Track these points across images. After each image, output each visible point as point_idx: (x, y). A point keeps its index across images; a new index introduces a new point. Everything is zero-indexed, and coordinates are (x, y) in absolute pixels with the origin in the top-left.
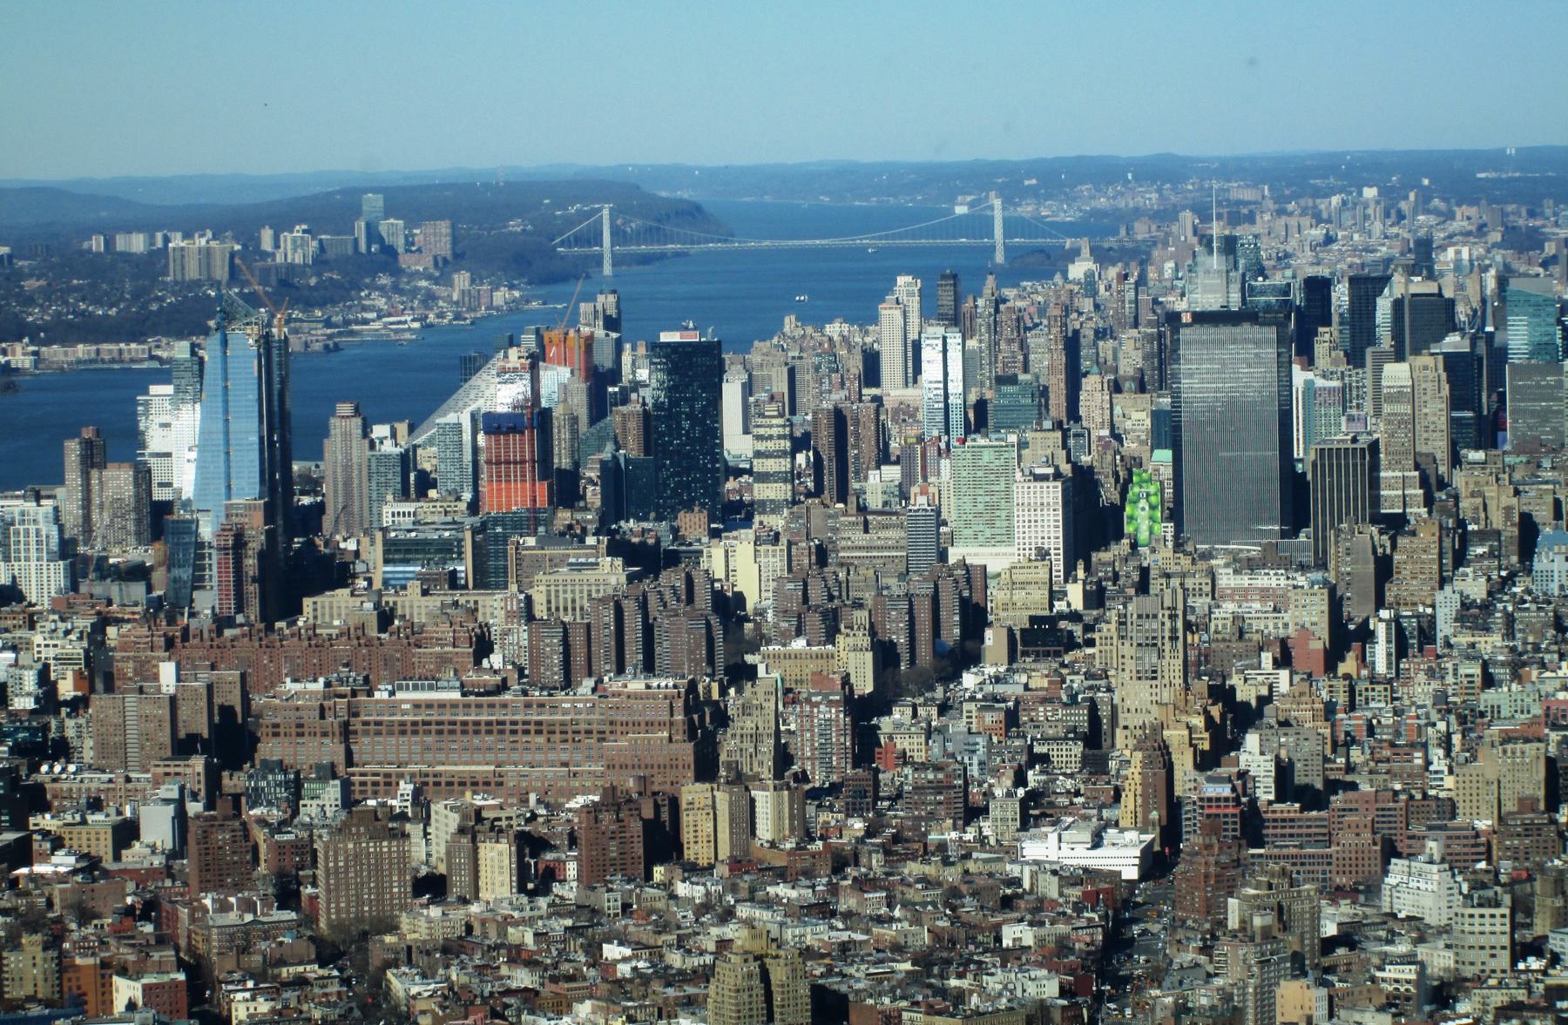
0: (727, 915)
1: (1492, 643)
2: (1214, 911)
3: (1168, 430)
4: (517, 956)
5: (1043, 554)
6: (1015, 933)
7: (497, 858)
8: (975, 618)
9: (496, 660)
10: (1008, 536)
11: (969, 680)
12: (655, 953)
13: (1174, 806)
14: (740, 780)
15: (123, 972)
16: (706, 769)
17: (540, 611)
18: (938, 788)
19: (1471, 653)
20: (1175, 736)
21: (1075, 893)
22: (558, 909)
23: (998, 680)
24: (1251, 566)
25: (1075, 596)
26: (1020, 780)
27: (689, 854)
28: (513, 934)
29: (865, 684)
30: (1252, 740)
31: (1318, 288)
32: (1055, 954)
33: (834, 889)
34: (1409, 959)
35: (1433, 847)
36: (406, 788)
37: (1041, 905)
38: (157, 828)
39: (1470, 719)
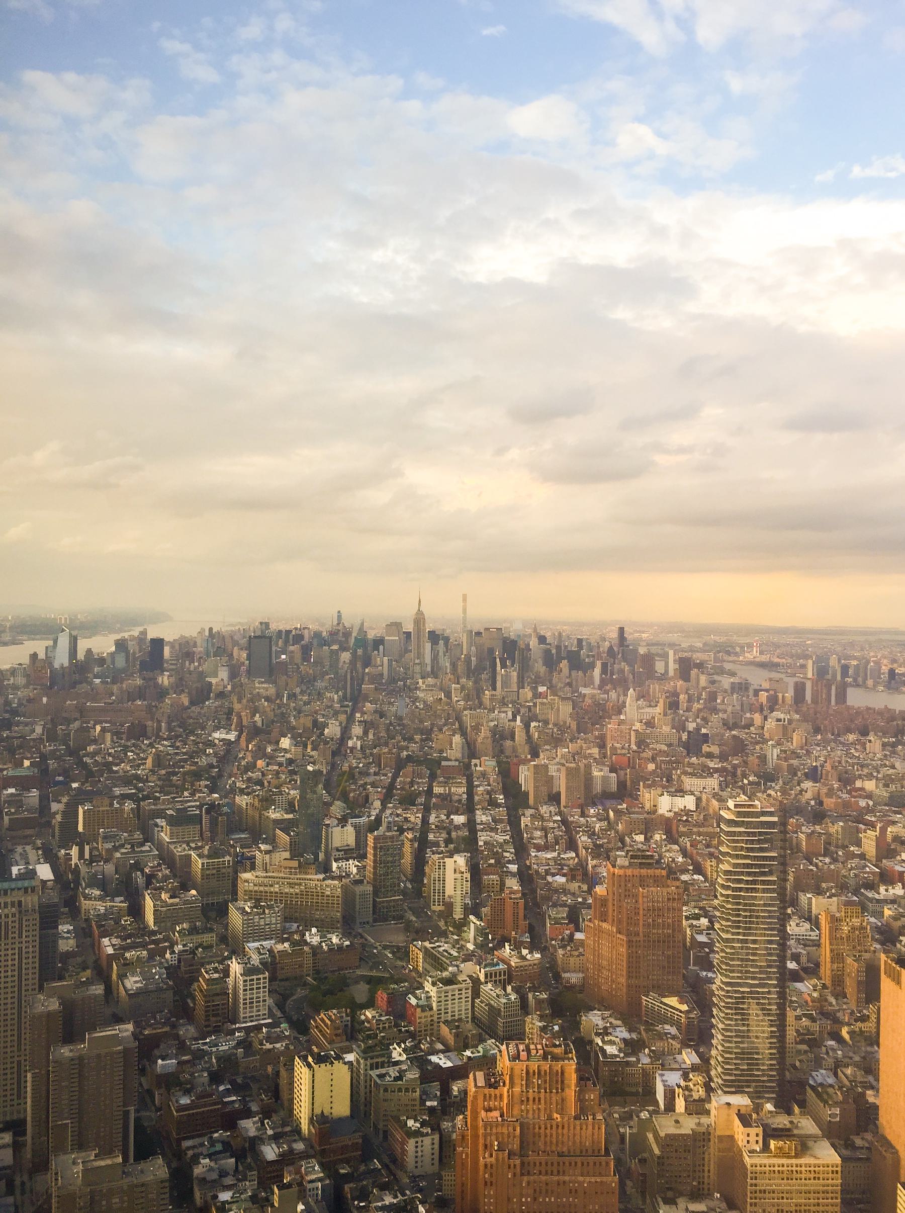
0: (154, 747)
1: (305, 698)
2: (248, 747)
3: (249, 657)
4: (110, 754)
5: (222, 680)
6: (210, 751)
7: (108, 736)
8: (210, 691)
9: (114, 698)
10: (217, 677)
11: (207, 703)
12: (138, 754)
13: (242, 726)
14: (159, 722)
15: (27, 759)
16: (152, 719)
17: (124, 689)
18: (197, 723)
19: (301, 700)
20: (243, 714)
21: (221, 743)
22: (119, 746)
23: (212, 703)
24: (262, 683)
25: (229, 688)
26: (214, 722)
27: (148, 734)
28: (110, 751)
29: (186, 703)
30: (257, 715)
31: (280, 631)
32: (215, 754)
33: (175, 742)
34: (283, 756)
35: (289, 735)
36: (92, 722)
37: (215, 745)
38: (39, 729)
39: (300, 712)
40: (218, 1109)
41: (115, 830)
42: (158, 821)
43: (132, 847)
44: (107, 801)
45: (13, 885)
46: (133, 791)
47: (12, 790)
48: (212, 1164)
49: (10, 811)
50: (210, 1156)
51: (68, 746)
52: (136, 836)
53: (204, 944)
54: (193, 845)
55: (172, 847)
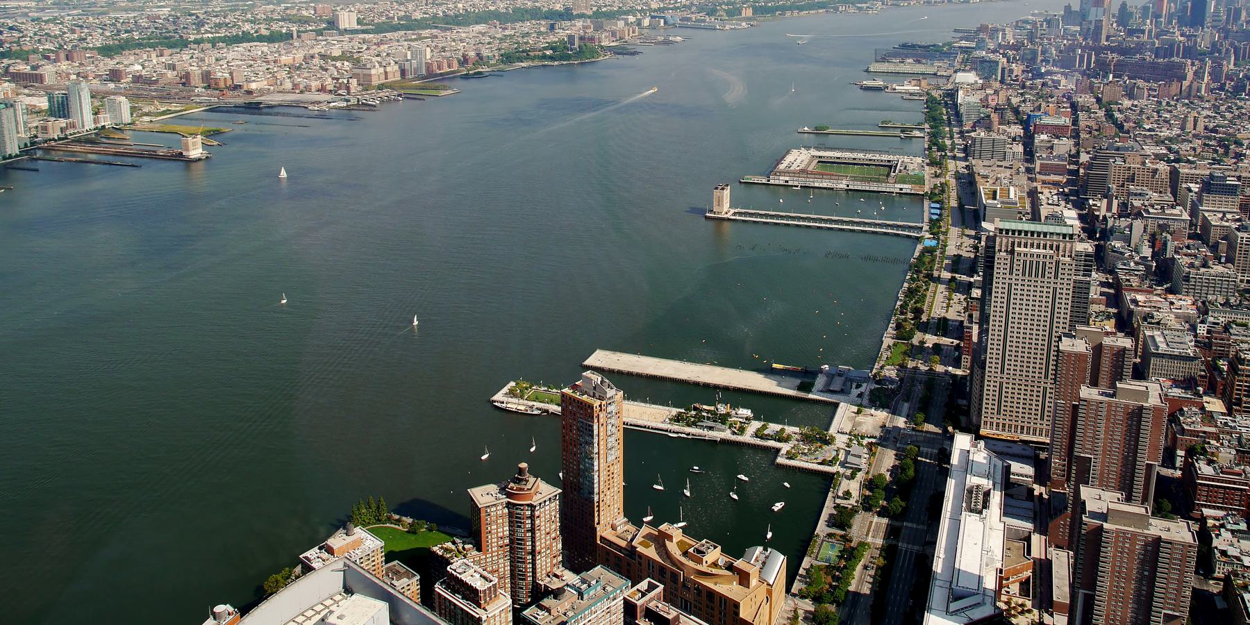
40: (1245, 489)
41: (1145, 188)
42: (1191, 185)
43: (1162, 208)
44: (1139, 159)
45: (1045, 228)
46: (1164, 152)
47: (1044, 137)
48: (1235, 540)
49: (1041, 156)
50: (1233, 532)
51: (1099, 100)
52: (1166, 198)
53: (1238, 320)
54: (1229, 216)
55: (1206, 214)
